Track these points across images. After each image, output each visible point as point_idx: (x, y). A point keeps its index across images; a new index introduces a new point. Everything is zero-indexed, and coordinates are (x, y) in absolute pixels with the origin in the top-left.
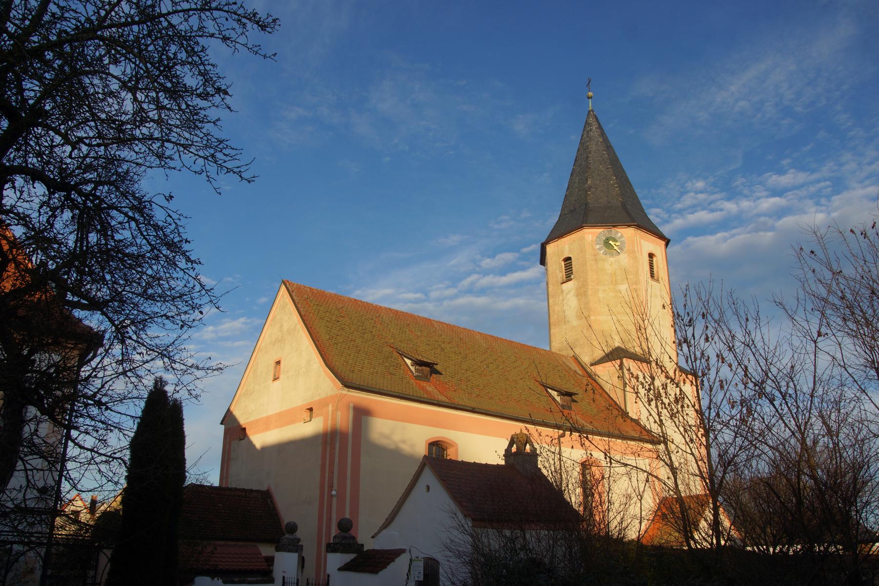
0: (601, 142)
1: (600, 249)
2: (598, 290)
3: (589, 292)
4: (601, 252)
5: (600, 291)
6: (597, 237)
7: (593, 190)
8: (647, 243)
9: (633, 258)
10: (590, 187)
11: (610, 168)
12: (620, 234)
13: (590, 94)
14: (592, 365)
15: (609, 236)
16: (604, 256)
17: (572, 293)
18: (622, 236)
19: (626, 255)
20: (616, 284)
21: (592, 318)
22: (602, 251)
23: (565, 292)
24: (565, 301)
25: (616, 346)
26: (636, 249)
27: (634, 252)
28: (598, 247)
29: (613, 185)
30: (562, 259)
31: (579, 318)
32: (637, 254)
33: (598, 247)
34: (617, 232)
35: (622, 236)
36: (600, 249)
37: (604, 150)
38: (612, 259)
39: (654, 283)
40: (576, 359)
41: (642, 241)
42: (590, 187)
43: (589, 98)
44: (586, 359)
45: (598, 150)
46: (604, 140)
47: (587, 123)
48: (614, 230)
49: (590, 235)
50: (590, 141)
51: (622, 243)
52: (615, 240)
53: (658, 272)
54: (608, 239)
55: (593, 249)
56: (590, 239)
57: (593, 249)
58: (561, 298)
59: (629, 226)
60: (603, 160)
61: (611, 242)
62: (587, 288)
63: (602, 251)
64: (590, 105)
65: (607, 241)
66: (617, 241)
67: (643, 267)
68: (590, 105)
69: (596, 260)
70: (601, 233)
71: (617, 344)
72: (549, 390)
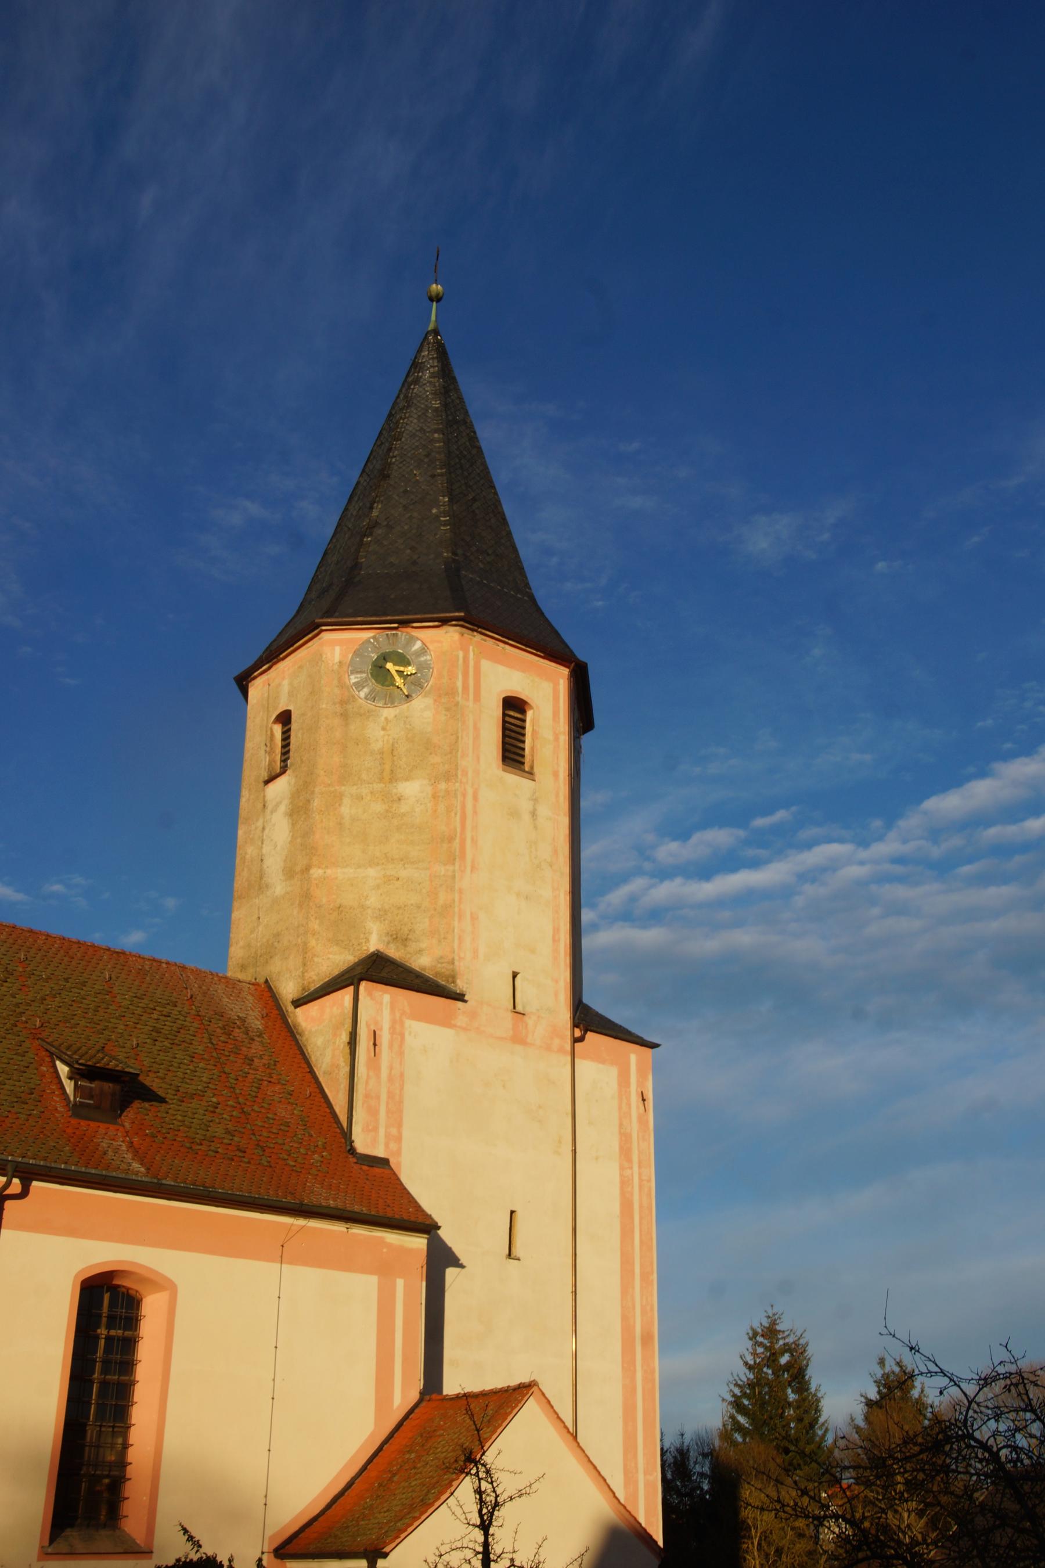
0: (436, 410)
1: (359, 686)
2: (340, 796)
3: (316, 803)
4: (362, 694)
5: (346, 801)
6: (356, 653)
7: (380, 531)
8: (501, 668)
9: (448, 709)
10: (375, 524)
11: (441, 475)
12: (418, 645)
13: (436, 288)
14: (298, 1003)
15: (387, 649)
16: (369, 705)
17: (283, 808)
18: (424, 650)
19: (429, 701)
20: (391, 781)
21: (316, 873)
22: (366, 690)
23: (270, 807)
24: (267, 831)
25: (372, 949)
26: (459, 684)
27: (452, 692)
28: (354, 679)
29: (437, 517)
30: (274, 717)
31: (289, 873)
32: (459, 699)
33: (354, 679)
34: (412, 640)
35: (424, 650)
36: (359, 686)
37: (436, 431)
38: (389, 713)
39: (512, 779)
40: (270, 988)
41: (486, 665)
42: (375, 524)
43: (431, 299)
44: (288, 989)
45: (422, 430)
46: (446, 405)
47: (416, 365)
48: (403, 634)
49: (337, 649)
50: (409, 406)
51: (421, 668)
52: (402, 660)
53: (532, 749)
54: (385, 658)
55: (342, 685)
56: (337, 658)
57: (342, 685)
58: (260, 824)
59: (444, 622)
60: (427, 456)
61: (389, 666)
62: (313, 793)
63: (366, 690)
64: (433, 318)
65: (381, 662)
66: (408, 663)
67: (476, 729)
68: (433, 318)
69: (345, 716)
70: (368, 641)
71: (374, 944)
72: (58, 1063)
